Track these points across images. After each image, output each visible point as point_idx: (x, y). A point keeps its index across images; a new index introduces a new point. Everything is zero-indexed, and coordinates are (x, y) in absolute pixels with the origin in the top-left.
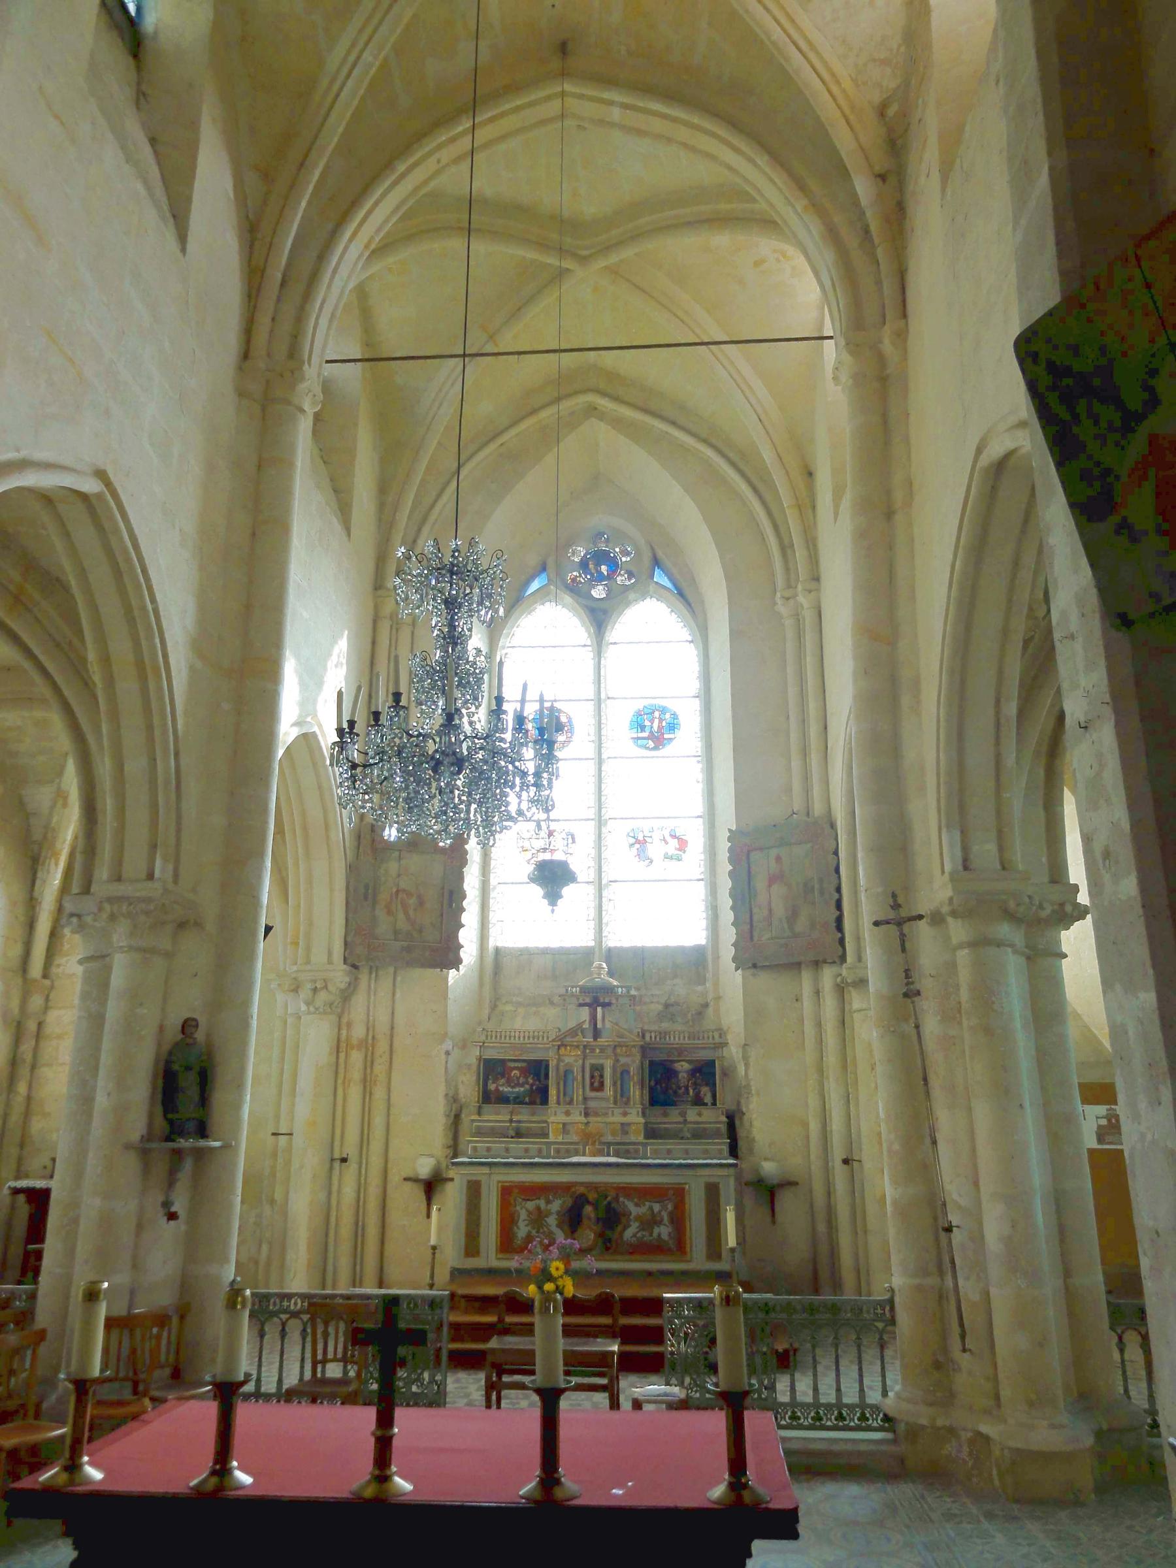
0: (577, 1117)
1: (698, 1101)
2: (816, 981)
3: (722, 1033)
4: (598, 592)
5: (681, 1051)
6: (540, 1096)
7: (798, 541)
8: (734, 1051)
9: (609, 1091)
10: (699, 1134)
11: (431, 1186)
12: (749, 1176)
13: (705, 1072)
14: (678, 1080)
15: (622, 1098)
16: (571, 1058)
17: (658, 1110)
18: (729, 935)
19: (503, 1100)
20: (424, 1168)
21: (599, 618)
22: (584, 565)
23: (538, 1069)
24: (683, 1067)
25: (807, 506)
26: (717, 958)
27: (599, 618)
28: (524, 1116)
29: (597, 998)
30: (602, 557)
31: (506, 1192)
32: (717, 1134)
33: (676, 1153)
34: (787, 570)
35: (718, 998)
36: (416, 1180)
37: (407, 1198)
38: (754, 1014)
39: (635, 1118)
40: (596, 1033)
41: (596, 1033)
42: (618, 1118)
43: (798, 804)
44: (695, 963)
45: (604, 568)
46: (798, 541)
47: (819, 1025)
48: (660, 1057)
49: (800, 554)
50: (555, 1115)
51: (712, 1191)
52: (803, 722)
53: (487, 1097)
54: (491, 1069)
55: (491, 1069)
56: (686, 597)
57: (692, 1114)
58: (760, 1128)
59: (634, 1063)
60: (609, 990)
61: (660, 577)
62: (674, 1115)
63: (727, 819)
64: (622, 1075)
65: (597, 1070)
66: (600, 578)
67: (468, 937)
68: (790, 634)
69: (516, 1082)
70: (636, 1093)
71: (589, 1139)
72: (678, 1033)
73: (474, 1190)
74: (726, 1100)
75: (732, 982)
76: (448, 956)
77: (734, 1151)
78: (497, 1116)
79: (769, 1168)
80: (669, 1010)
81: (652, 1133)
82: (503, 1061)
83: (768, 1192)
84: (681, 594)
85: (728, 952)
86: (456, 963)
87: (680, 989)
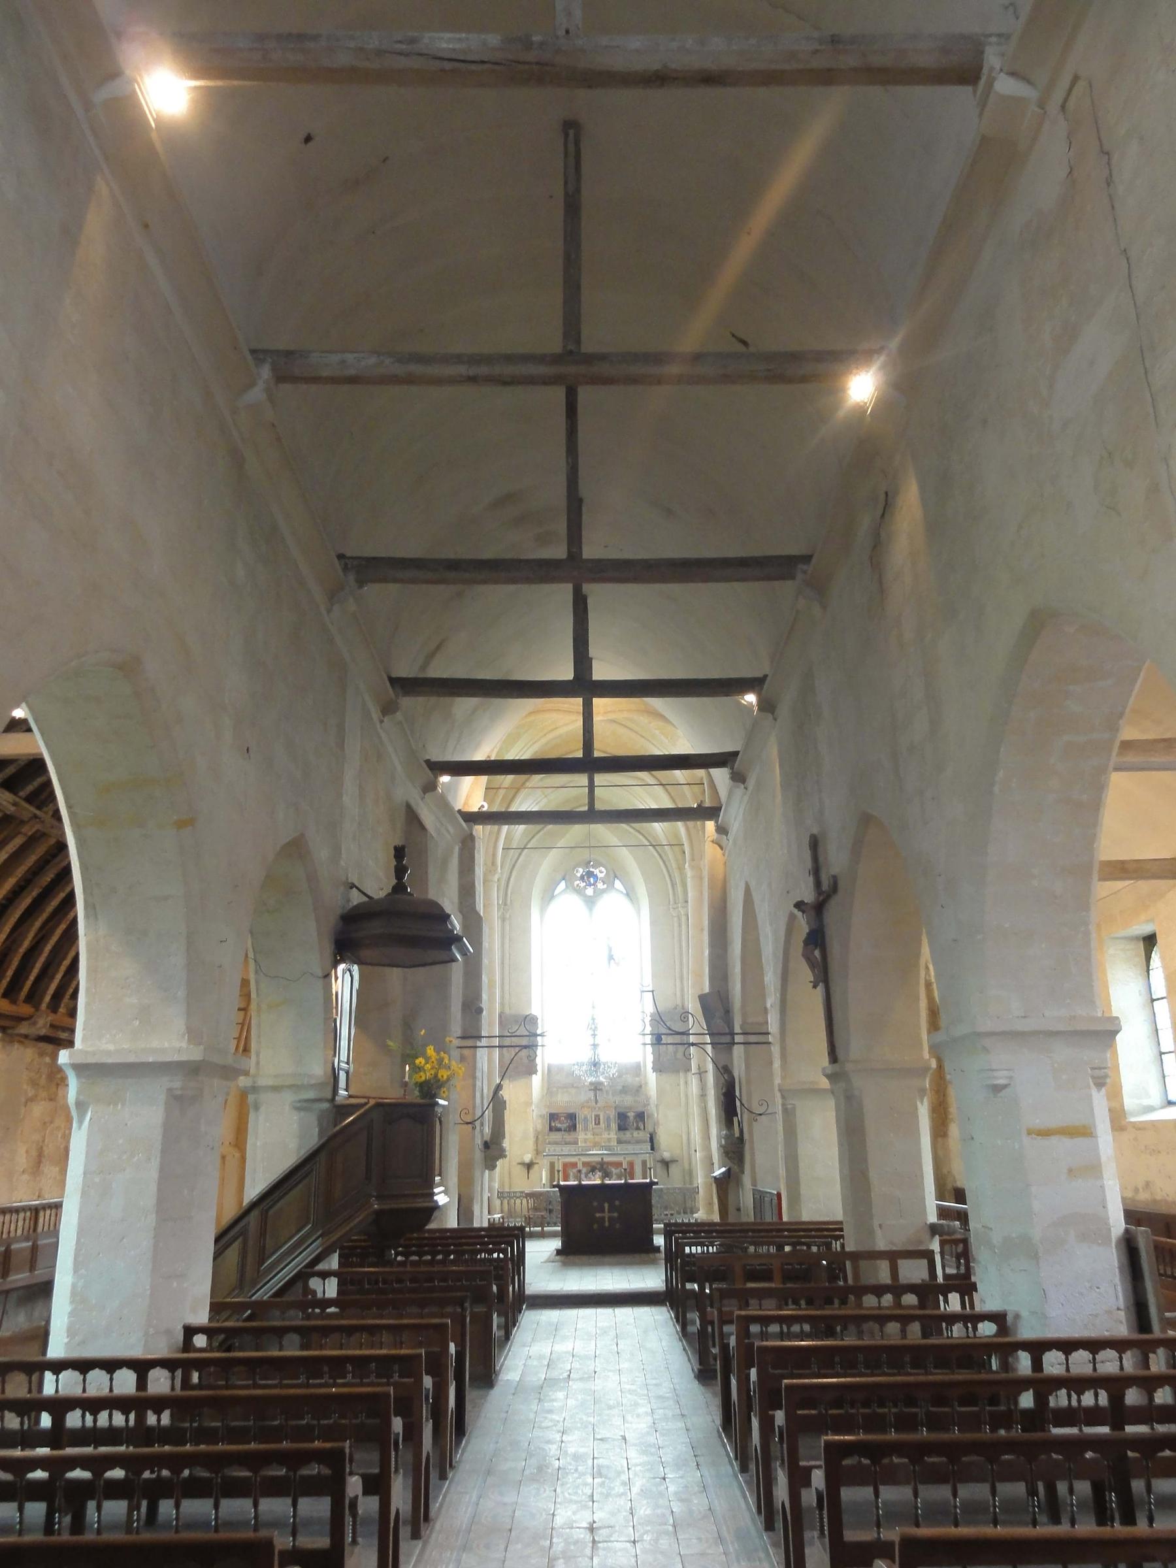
0: (589, 1136)
1: (638, 1128)
2: (686, 1077)
3: (648, 1099)
4: (590, 891)
5: (630, 1108)
6: (573, 1128)
7: (678, 881)
8: (652, 1108)
9: (602, 1125)
10: (638, 1142)
11: (529, 1166)
12: (658, 1158)
13: (641, 1116)
14: (632, 1120)
15: (608, 1127)
16: (586, 1112)
17: (622, 1133)
18: (650, 1058)
19: (559, 1130)
20: (527, 1158)
21: (590, 902)
22: (582, 878)
23: (572, 1117)
24: (631, 1115)
25: (681, 869)
26: (645, 1066)
27: (590, 902)
28: (568, 1137)
29: (596, 1088)
30: (590, 874)
31: (565, 1165)
32: (645, 1142)
33: (630, 1148)
34: (674, 894)
35: (646, 1083)
36: (523, 1164)
37: (520, 1171)
38: (661, 1091)
39: (613, 1136)
40: (596, 1102)
41: (596, 1102)
42: (605, 1136)
43: (679, 1002)
44: (637, 1069)
45: (592, 880)
46: (678, 881)
47: (687, 1096)
48: (622, 1110)
49: (679, 889)
50: (582, 1136)
51: (644, 1163)
52: (681, 964)
53: (551, 1129)
54: (553, 1117)
55: (553, 1117)
56: (630, 894)
57: (635, 1134)
58: (663, 1139)
59: (613, 1114)
60: (601, 1083)
61: (617, 882)
62: (628, 1135)
63: (650, 1009)
64: (608, 1119)
65: (597, 1117)
66: (590, 885)
67: (538, 1060)
68: (676, 924)
69: (562, 1123)
70: (614, 1126)
71: (596, 1145)
72: (628, 1100)
73: (552, 1165)
74: (650, 1128)
75: (652, 1077)
76: (531, 1070)
77: (652, 1149)
78: (556, 1136)
79: (667, 1155)
80: (625, 1090)
81: (619, 1142)
82: (557, 1114)
83: (666, 1164)
84: (628, 895)
85: (650, 1065)
86: (535, 1072)
87: (630, 1079)
